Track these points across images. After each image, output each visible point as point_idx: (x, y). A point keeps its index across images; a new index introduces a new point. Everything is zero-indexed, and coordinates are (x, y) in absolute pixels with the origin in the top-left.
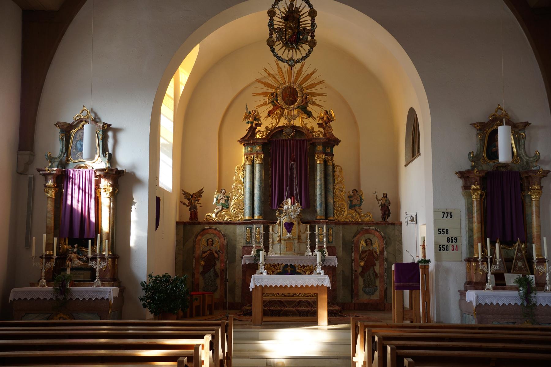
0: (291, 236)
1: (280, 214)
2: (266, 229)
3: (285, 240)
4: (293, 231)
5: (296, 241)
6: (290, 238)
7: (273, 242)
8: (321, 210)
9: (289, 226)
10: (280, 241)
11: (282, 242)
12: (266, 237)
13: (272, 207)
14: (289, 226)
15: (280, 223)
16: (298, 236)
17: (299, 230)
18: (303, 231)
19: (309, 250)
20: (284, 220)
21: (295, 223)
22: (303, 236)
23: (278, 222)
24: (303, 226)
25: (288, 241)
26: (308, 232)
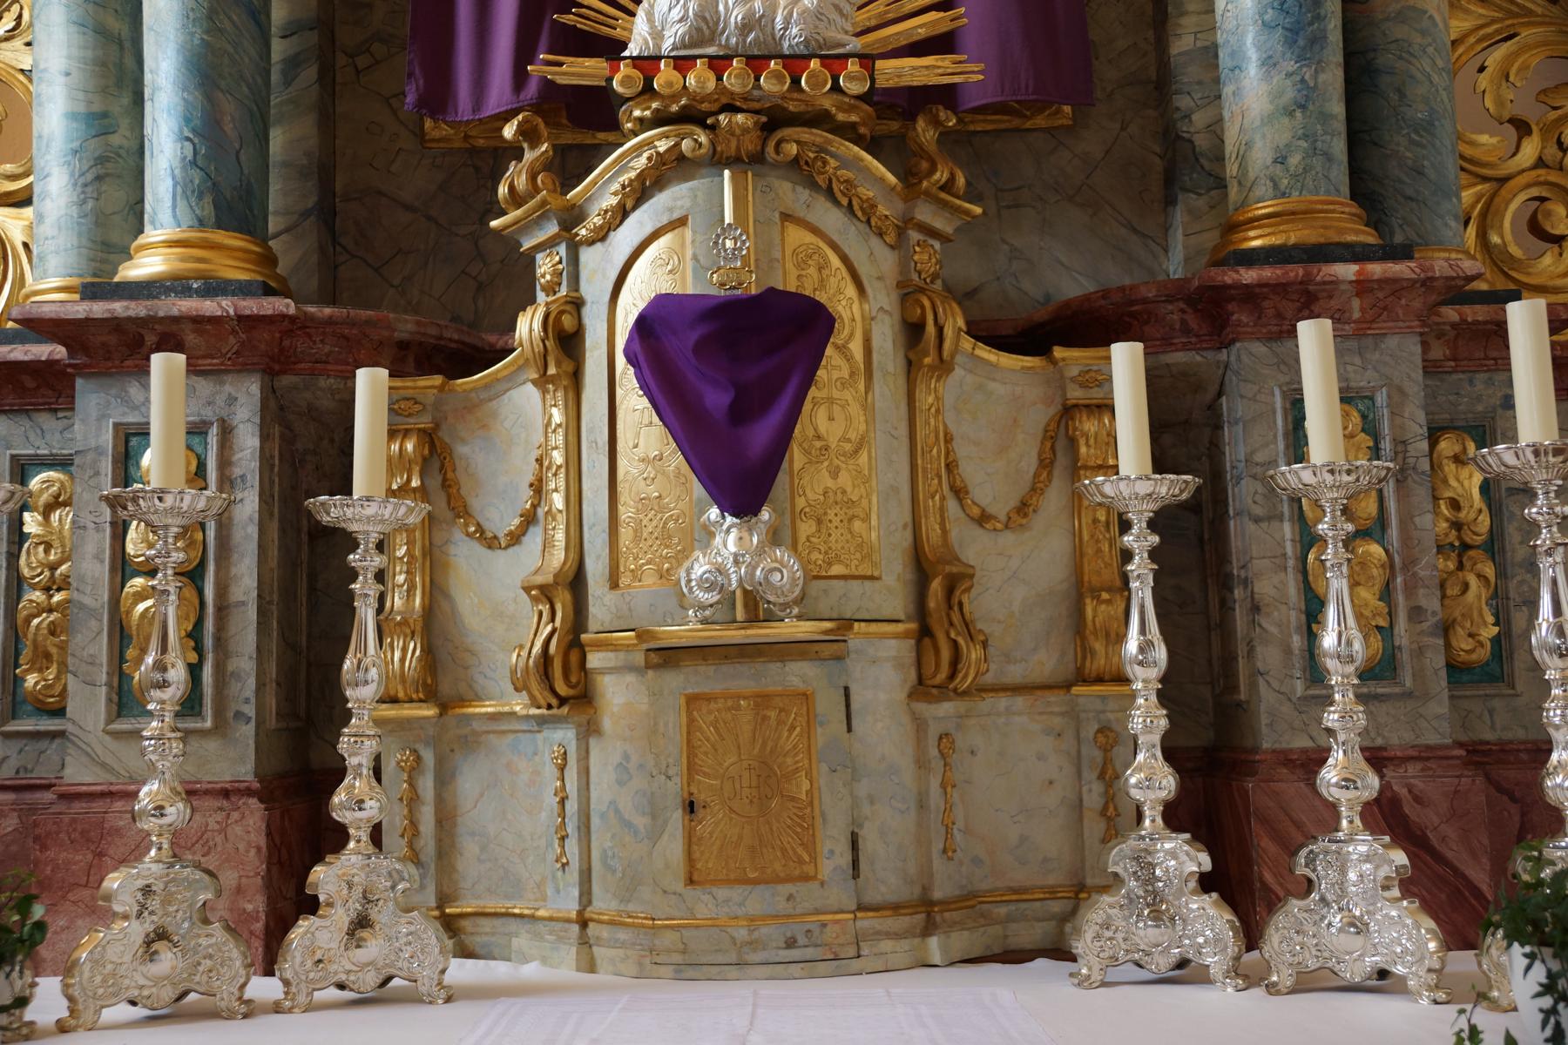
0: (782, 571)
1: (571, 166)
2: (310, 453)
3: (667, 656)
4: (806, 476)
5: (881, 669)
6: (755, 606)
7: (440, 678)
8: (1305, 101)
9: (734, 375)
10: (565, 682)
11: (620, 693)
12: (311, 583)
13: (437, 99)
14: (734, 375)
15: (566, 341)
16: (922, 567)
17: (934, 469)
18: (993, 479)
19: (1181, 858)
20: (643, 254)
21: (863, 318)
22: (1014, 578)
23: (528, 325)
24: (994, 395)
25: (733, 653)
26: (1132, 473)
